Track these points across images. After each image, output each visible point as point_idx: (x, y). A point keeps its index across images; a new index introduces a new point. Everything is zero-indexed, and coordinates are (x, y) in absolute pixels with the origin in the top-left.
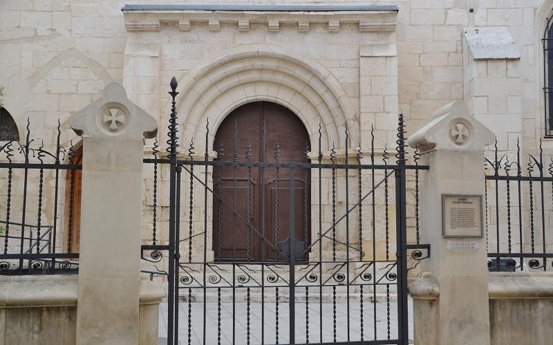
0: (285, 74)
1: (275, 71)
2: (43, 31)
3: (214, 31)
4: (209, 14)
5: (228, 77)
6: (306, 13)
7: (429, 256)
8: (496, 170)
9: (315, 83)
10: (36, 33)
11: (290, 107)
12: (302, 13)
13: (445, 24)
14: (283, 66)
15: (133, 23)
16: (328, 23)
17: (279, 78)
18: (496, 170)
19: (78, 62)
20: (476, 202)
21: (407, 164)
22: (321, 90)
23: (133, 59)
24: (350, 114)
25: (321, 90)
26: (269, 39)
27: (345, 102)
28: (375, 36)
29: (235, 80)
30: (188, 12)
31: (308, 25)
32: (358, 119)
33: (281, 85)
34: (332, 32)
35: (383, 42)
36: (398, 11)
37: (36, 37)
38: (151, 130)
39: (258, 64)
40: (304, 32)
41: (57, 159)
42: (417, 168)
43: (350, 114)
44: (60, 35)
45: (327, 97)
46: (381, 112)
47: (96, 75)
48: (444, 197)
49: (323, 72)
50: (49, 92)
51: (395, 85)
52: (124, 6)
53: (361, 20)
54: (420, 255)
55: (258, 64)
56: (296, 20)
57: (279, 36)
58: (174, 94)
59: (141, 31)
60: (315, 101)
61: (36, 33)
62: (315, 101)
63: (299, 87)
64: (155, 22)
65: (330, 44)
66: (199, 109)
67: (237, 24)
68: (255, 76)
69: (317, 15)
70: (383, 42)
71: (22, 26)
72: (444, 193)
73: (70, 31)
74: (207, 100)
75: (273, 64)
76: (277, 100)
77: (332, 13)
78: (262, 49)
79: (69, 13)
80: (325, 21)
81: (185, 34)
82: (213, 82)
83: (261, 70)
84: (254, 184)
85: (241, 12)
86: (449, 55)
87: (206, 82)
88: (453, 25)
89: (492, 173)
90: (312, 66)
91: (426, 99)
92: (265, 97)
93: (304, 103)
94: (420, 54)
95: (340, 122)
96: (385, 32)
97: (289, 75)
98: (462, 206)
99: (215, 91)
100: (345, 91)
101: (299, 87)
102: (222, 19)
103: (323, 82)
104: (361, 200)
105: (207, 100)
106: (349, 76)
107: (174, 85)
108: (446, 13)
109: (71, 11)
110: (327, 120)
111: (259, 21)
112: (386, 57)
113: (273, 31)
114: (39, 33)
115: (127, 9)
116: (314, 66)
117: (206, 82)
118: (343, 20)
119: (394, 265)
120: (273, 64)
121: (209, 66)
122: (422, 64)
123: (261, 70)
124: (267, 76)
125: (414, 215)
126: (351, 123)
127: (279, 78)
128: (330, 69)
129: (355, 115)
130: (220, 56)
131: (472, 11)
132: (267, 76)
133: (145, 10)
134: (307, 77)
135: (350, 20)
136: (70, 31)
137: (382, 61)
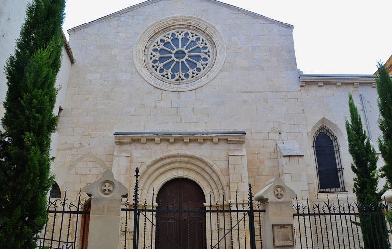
1: (187, 163)
2: (77, 145)
3: (157, 144)
5: (164, 166)
8: (298, 211)
9: (207, 169)
10: (73, 146)
11: (195, 180)
12: (200, 135)
14: (191, 161)
16: (212, 140)
17: (189, 166)
18: (298, 211)
20: (289, 228)
21: (254, 209)
22: (210, 172)
24: (225, 184)
25: (210, 172)
26: (184, 147)
27: (222, 177)
28: (235, 145)
29: (167, 167)
30: (145, 135)
32: (229, 186)
33: (190, 170)
34: (215, 144)
35: (240, 148)
37: (73, 147)
38: (125, 194)
39: (179, 159)
40: (201, 144)
41: (78, 208)
42: (259, 211)
43: (225, 184)
44: (84, 146)
45: (213, 175)
47: (99, 165)
48: (274, 226)
49: (211, 163)
50: (76, 174)
51: (246, 168)
57: (189, 145)
58: (137, 176)
60: (207, 177)
61: (73, 146)
62: (207, 177)
63: (199, 170)
65: (214, 149)
66: (149, 181)
67: (168, 140)
68: (177, 165)
74: (153, 178)
75: (186, 159)
77: (214, 135)
78: (181, 152)
81: (143, 145)
83: (180, 162)
84: (177, 220)
87: (153, 168)
89: (296, 212)
90: (205, 160)
93: (202, 178)
95: (220, 187)
96: (240, 143)
97: (194, 165)
98: (282, 230)
99: (157, 173)
101: (199, 170)
102: (161, 138)
103: (211, 168)
105: (153, 178)
106: (224, 165)
107: (137, 171)
109: (90, 135)
110: (213, 186)
111: (180, 138)
113: (186, 144)
114: (75, 146)
115: (116, 134)
116: (206, 160)
117: (153, 168)
118: (220, 138)
120: (186, 159)
123: (180, 162)
124: (183, 165)
125: (259, 234)
126: (225, 188)
127: (189, 166)
129: (227, 184)
131: (280, 133)
132: (183, 165)
133: (125, 134)
134: (203, 166)
137: (239, 157)
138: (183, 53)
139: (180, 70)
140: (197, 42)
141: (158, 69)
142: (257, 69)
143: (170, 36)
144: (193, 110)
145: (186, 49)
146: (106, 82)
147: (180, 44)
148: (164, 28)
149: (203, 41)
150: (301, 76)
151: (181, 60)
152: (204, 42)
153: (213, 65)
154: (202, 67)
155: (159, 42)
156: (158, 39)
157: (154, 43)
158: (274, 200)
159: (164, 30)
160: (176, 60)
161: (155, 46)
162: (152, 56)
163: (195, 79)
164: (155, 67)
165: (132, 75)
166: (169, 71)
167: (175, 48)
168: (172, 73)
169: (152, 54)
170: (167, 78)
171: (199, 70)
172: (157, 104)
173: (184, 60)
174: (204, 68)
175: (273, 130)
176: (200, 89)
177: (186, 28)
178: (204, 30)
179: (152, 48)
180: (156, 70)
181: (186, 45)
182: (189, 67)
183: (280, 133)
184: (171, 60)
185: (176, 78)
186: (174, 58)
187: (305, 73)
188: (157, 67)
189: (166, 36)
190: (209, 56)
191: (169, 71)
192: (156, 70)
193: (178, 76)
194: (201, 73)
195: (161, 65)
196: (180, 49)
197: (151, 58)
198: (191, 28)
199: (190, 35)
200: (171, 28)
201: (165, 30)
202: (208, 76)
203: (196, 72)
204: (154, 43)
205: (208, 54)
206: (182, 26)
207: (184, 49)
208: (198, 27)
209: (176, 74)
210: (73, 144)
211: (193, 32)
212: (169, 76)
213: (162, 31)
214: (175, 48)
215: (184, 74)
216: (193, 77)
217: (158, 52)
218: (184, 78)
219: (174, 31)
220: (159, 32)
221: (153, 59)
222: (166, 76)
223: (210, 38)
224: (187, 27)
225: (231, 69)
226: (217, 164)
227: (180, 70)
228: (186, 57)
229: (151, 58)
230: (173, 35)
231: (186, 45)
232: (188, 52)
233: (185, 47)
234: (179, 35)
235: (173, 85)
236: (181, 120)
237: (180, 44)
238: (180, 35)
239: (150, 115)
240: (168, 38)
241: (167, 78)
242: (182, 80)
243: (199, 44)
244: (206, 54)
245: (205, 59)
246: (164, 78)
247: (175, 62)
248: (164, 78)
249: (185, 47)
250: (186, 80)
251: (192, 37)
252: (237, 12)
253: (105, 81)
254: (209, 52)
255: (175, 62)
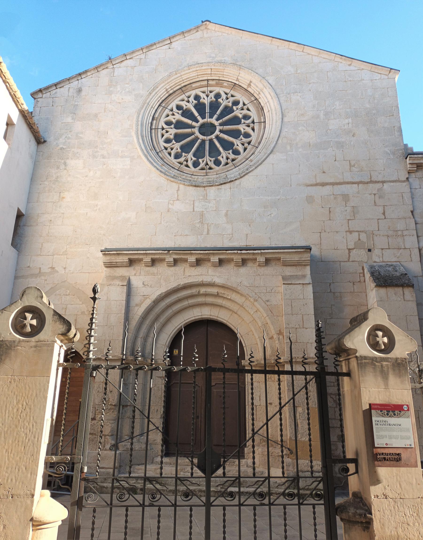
0: (224, 298)
1: (217, 295)
4: (166, 253)
6: (239, 252)
7: (357, 472)
10: (40, 271)
11: (228, 324)
12: (236, 252)
13: (349, 261)
14: (221, 291)
15: (109, 261)
16: (256, 259)
19: (68, 291)
23: (107, 287)
31: (241, 260)
33: (221, 306)
36: (311, 249)
39: (203, 290)
44: (57, 272)
46: (300, 328)
52: (103, 249)
53: (282, 256)
54: (347, 470)
55: (203, 290)
56: (232, 257)
57: (219, 269)
59: (115, 267)
61: (40, 271)
64: (125, 259)
69: (248, 253)
70: (300, 273)
71: (31, 266)
72: (370, 402)
73: (65, 268)
75: (214, 290)
76: (218, 319)
77: (259, 251)
78: (207, 279)
79: (65, 256)
80: (254, 257)
82: (168, 304)
85: (189, 252)
86: (354, 284)
88: (355, 261)
91: (337, 318)
92: (209, 317)
94: (330, 283)
97: (227, 299)
100: (271, 311)
104: (281, 408)
108: (349, 253)
109: (66, 255)
112: (303, 284)
115: (106, 252)
118: (267, 256)
119: (320, 482)
121: (165, 292)
122: (332, 291)
124: (210, 300)
126: (275, 336)
128: (258, 294)
130: (173, 285)
131: (370, 250)
132: (210, 300)
133: (118, 252)
135: (274, 256)
136: (65, 268)
137: (300, 287)
138: (213, 127)
139: (207, 153)
140: (235, 108)
141: (173, 153)
142: (332, 147)
143: (192, 99)
144: (226, 215)
145: (217, 120)
146: (91, 174)
147: (207, 110)
148: (183, 85)
149: (244, 104)
150: (408, 153)
151: (209, 137)
152: (245, 107)
153: (259, 143)
154: (241, 148)
155: (175, 109)
156: (173, 105)
157: (167, 111)
158: (370, 355)
159: (183, 89)
160: (201, 137)
161: (168, 116)
162: (164, 131)
163: (230, 167)
164: (169, 150)
165: (131, 162)
166: (190, 156)
167: (199, 118)
168: (194, 159)
169: (163, 129)
170: (187, 166)
171: (236, 152)
172: (170, 206)
173: (213, 136)
174: (245, 149)
175: (359, 245)
176: (237, 182)
177: (217, 85)
178: (245, 87)
179: (163, 120)
180: (170, 154)
181: (218, 112)
182: (221, 149)
183: (370, 250)
184: (193, 137)
185: (200, 167)
186: (197, 134)
187: (415, 150)
188: (172, 149)
189: (186, 99)
190: (253, 129)
191: (190, 156)
192: (170, 154)
193: (205, 162)
194: (240, 157)
195: (177, 146)
196: (208, 120)
197: (163, 136)
198: (225, 84)
199: (224, 96)
200: (194, 85)
201: (182, 89)
202: (251, 161)
203: (232, 156)
204: (167, 111)
205: (252, 125)
206: (210, 82)
207: (213, 120)
208: (237, 83)
209: (200, 160)
210: (40, 268)
211: (227, 91)
212: (190, 164)
213: (180, 91)
214: (199, 118)
215: (213, 159)
216: (227, 164)
217: (172, 126)
218: (213, 166)
219: (198, 92)
220: (175, 92)
221: (164, 137)
222: (185, 163)
223: (256, 99)
224: (219, 82)
225: (288, 148)
226: (263, 298)
227: (207, 153)
228: (217, 132)
229: (163, 136)
230: (197, 97)
231: (218, 112)
232: (221, 125)
233: (215, 116)
234: (206, 98)
235: (196, 177)
236: (208, 231)
237: (207, 110)
238: (207, 96)
239: (161, 223)
240: (188, 102)
241: (187, 166)
242: (210, 168)
243: (238, 113)
244: (248, 126)
245: (247, 135)
246: (183, 166)
247: (199, 141)
248: (183, 166)
249: (215, 116)
250: (217, 168)
251: (227, 98)
252: (302, 53)
253: (90, 170)
254: (253, 122)
255: (199, 141)
